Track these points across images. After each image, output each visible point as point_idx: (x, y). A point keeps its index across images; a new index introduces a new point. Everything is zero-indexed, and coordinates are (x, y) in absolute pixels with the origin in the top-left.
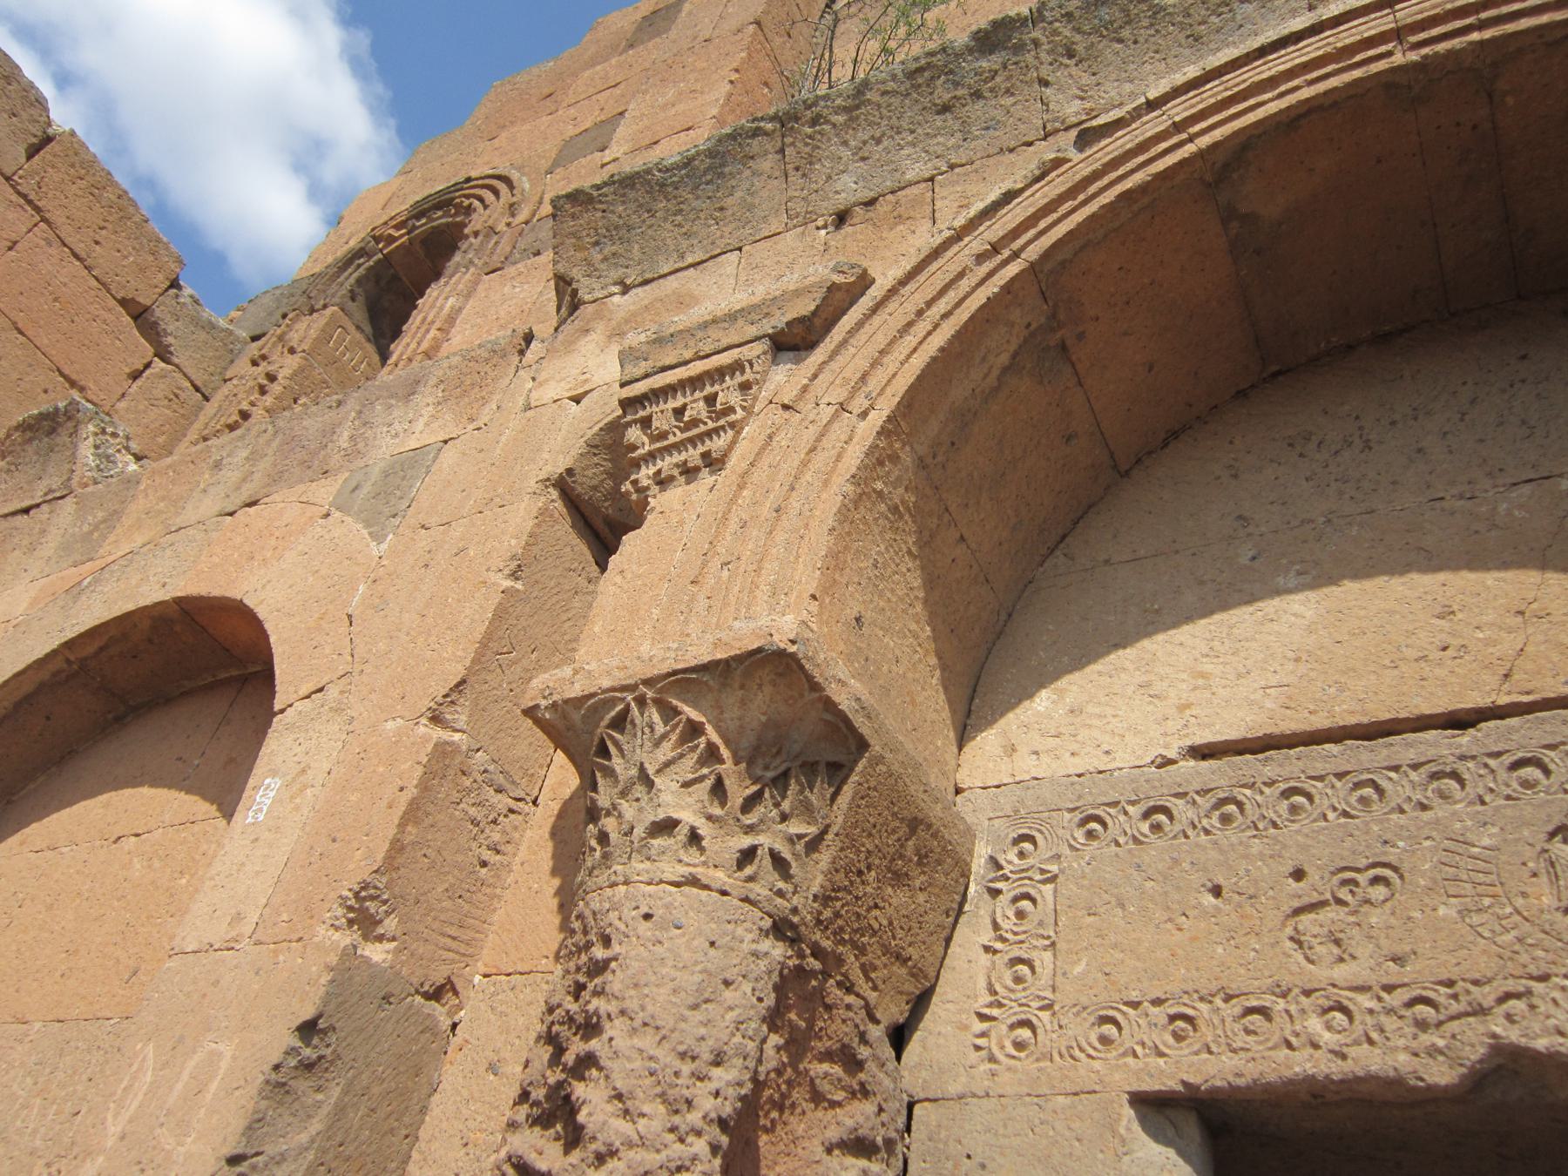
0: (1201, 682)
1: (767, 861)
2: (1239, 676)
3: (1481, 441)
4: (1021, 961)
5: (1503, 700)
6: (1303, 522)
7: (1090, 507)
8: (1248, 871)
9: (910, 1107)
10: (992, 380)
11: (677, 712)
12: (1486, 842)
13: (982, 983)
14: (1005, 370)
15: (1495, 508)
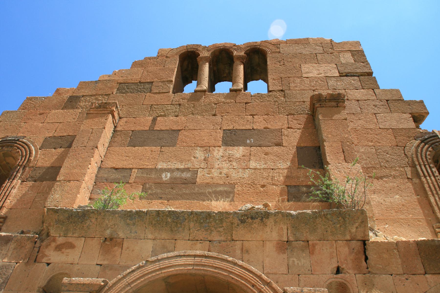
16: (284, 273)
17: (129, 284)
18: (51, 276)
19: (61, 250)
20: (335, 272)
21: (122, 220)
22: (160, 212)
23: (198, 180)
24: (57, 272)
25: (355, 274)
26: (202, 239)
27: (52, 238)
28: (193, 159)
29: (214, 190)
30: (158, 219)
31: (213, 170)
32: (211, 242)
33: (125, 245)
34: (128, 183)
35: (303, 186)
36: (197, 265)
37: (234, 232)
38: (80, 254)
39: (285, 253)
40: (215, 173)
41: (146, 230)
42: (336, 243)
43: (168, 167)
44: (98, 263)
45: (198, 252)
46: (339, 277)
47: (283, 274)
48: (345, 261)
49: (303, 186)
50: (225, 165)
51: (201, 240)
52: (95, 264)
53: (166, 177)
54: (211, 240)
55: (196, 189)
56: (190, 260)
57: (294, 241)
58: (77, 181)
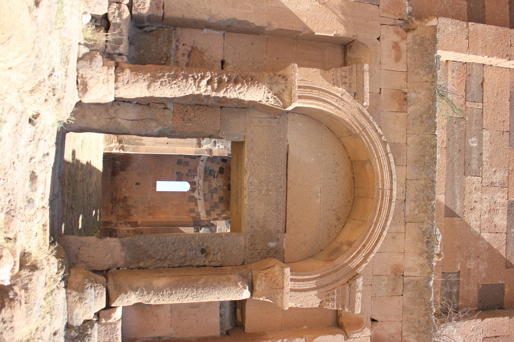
17: (364, 129)
19: (393, 48)
20: (373, 318)
21: (426, 109)
22: (435, 148)
23: (469, 177)
26: (408, 192)
27: (404, 36)
28: (494, 170)
29: (457, 195)
30: (428, 147)
31: (479, 193)
33: (400, 115)
34: (466, 101)
35: (458, 288)
36: (383, 193)
37: (414, 224)
39: (392, 273)
40: (476, 196)
41: (416, 135)
43: (484, 143)
44: (382, 90)
45: (395, 192)
48: (382, 328)
49: (458, 288)
50: (485, 206)
51: (406, 192)
52: (381, 87)
53: (473, 142)
54: (406, 202)
55: (458, 177)
56: (387, 186)
58: (468, 47)
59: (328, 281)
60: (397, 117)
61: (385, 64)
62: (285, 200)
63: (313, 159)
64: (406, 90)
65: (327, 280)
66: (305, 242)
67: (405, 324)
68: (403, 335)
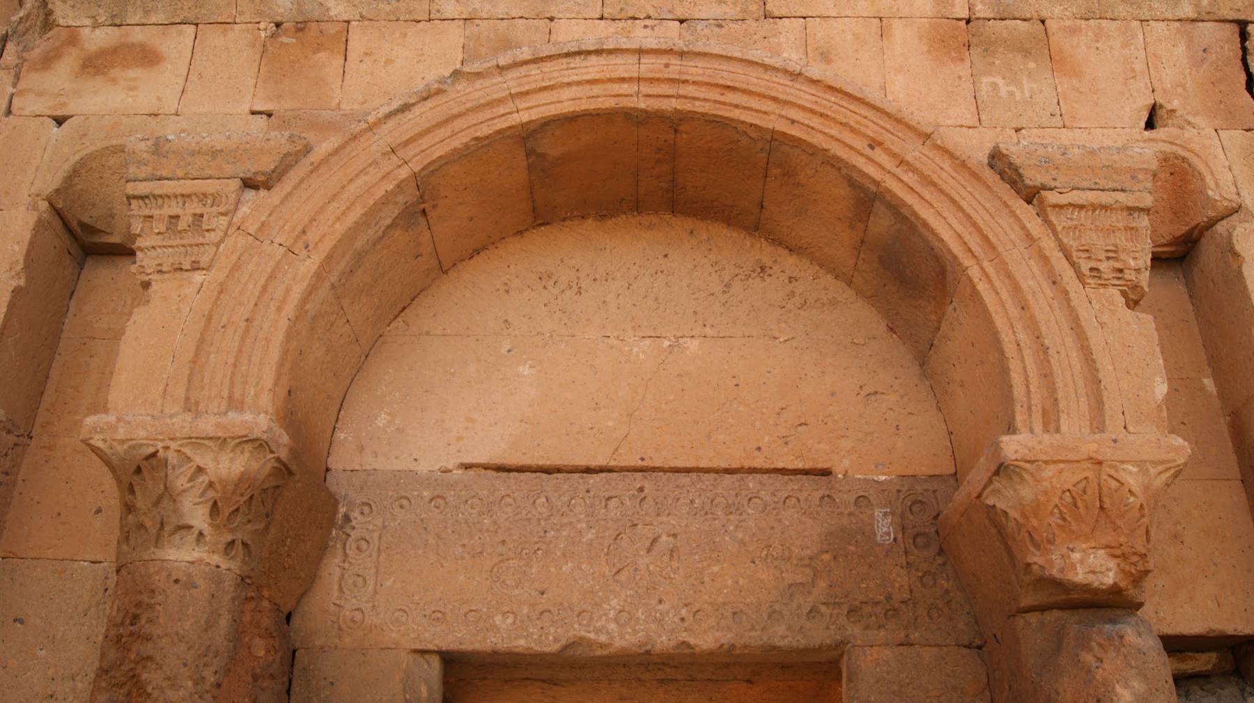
0: (470, 425)
1: (240, 547)
2: (491, 425)
3: (635, 305)
4: (359, 576)
5: (612, 463)
6: (538, 333)
7: (421, 291)
8: (480, 538)
9: (294, 651)
10: (380, 233)
11: (189, 459)
12: (590, 536)
13: (336, 587)
14: (388, 227)
15: (632, 350)
16: (963, 123)
18: (77, 157)
19: (105, 74)
24: (99, 146)
25: (1216, 130)
27: (64, 34)
32: (685, 25)
33: (357, 43)
38: (181, 81)
39: (962, 60)
42: (1145, 28)
44: (258, 108)
46: (1164, 138)
47: (962, 126)
51: (649, 17)
52: (247, 110)
54: (687, 16)
56: (624, 66)
57: (995, 19)
59: (1034, 277)
60: (366, 54)
61: (159, 99)
62: (694, 475)
63: (525, 370)
64: (267, 27)
65: (1031, 283)
66: (863, 393)
67: (1151, 9)
68: (1192, 15)
